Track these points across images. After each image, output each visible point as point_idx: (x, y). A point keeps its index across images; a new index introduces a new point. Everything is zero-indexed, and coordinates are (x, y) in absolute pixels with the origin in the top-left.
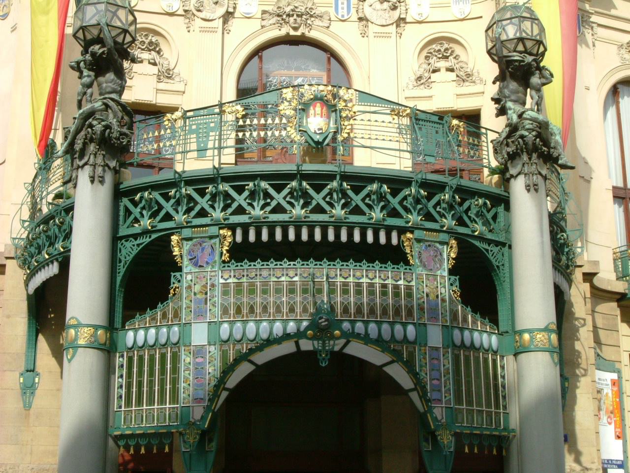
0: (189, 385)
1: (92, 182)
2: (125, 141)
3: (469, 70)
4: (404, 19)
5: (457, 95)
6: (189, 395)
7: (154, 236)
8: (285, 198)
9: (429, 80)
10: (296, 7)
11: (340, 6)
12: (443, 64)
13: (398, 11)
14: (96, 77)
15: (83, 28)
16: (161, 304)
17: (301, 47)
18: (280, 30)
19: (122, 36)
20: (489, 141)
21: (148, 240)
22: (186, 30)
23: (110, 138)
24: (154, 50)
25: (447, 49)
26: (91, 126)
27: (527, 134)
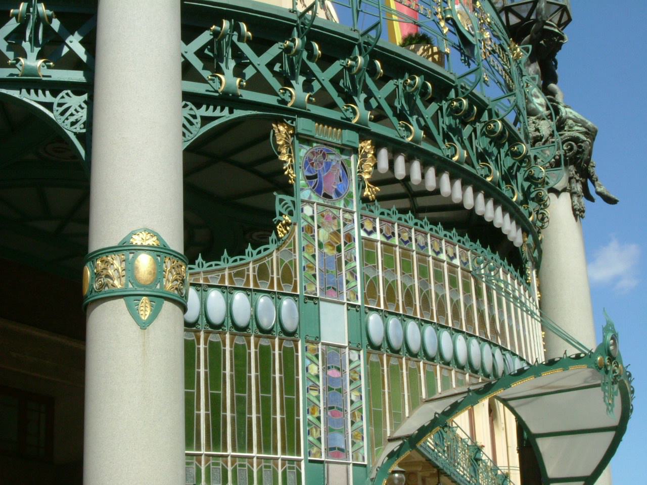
0: (319, 418)
6: (319, 439)
7: (239, 113)
16: (254, 248)
21: (225, 115)
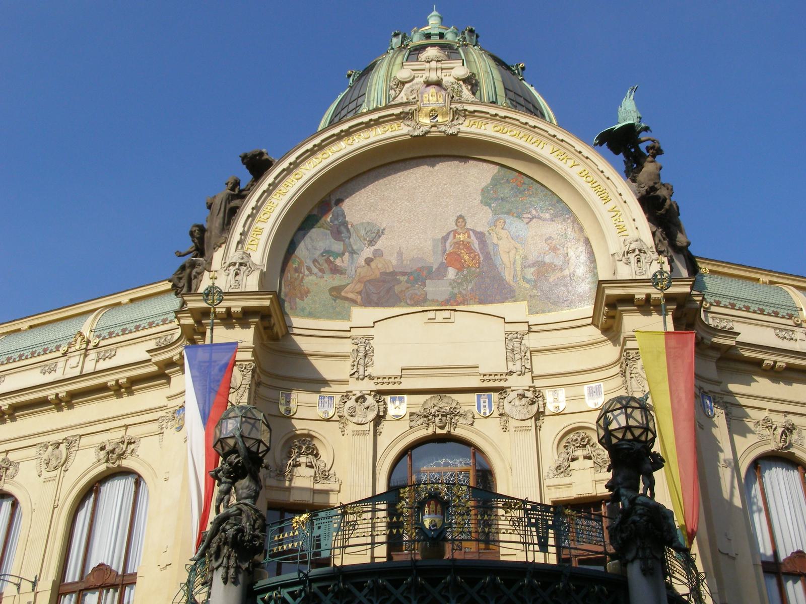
1: (225, 583)
2: (257, 543)
4: (542, 413)
5: (595, 481)
8: (402, 594)
9: (569, 468)
12: (580, 453)
13: (536, 404)
14: (233, 484)
15: (221, 441)
17: (449, 444)
18: (427, 429)
19: (257, 446)
20: (605, 528)
22: (341, 434)
23: (243, 541)
24: (311, 453)
25: (583, 439)
26: (224, 530)
27: (638, 519)
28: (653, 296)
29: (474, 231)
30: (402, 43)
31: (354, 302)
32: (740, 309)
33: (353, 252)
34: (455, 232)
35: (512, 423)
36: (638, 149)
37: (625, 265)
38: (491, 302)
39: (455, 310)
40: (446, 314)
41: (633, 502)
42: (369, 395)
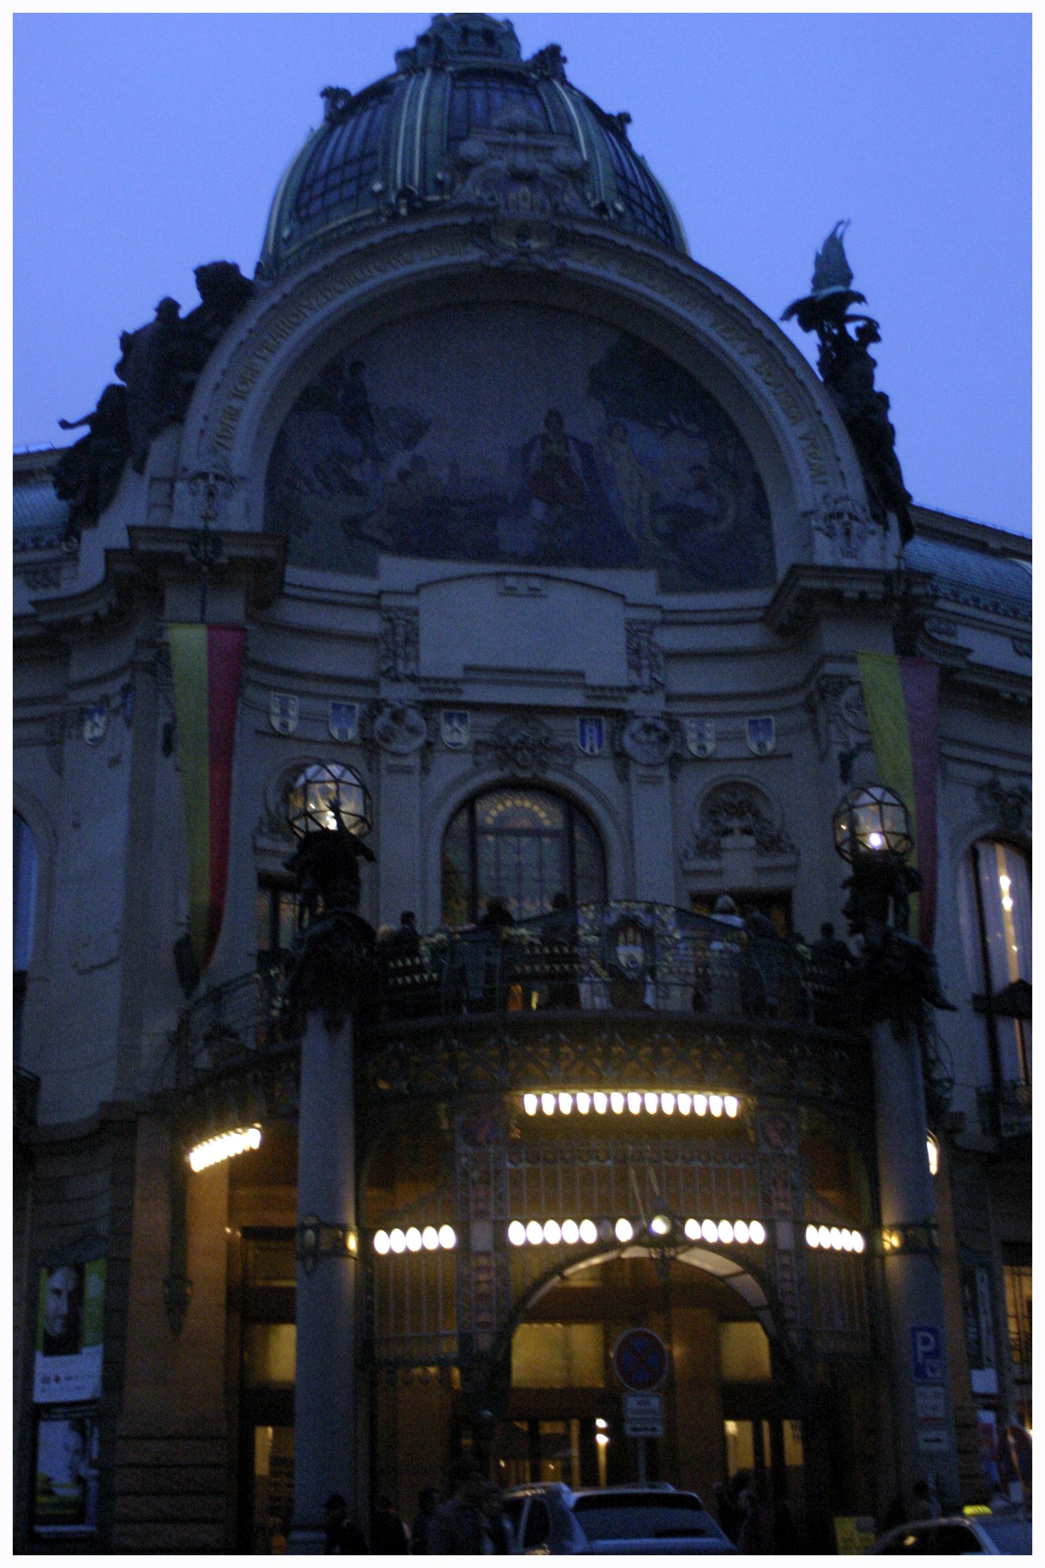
3: (774, 833)
10: (525, 737)
11: (587, 733)
12: (735, 823)
28: (871, 596)
29: (576, 441)
30: (436, 58)
31: (384, 548)
32: (966, 603)
33: (378, 458)
34: (545, 438)
35: (636, 771)
36: (843, 332)
37: (826, 541)
38: (602, 565)
39: (547, 577)
40: (535, 583)
41: (887, 936)
42: (410, 707)
